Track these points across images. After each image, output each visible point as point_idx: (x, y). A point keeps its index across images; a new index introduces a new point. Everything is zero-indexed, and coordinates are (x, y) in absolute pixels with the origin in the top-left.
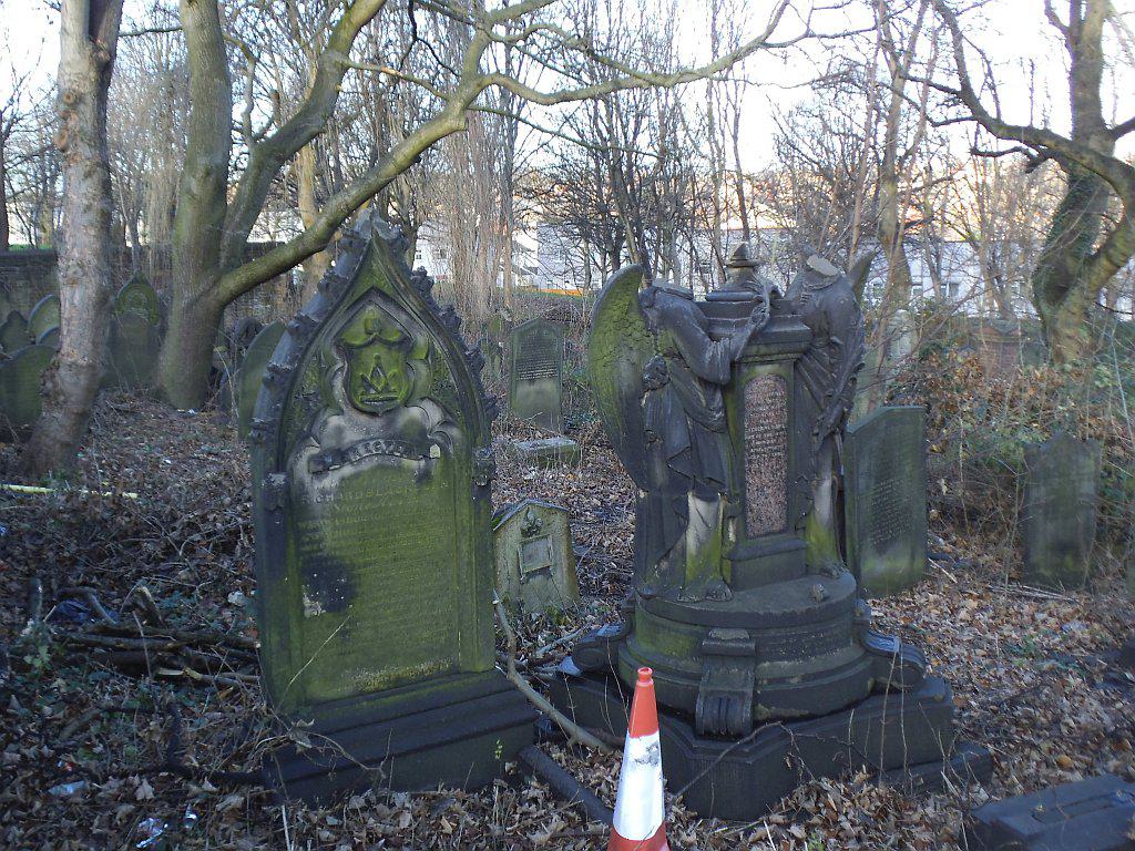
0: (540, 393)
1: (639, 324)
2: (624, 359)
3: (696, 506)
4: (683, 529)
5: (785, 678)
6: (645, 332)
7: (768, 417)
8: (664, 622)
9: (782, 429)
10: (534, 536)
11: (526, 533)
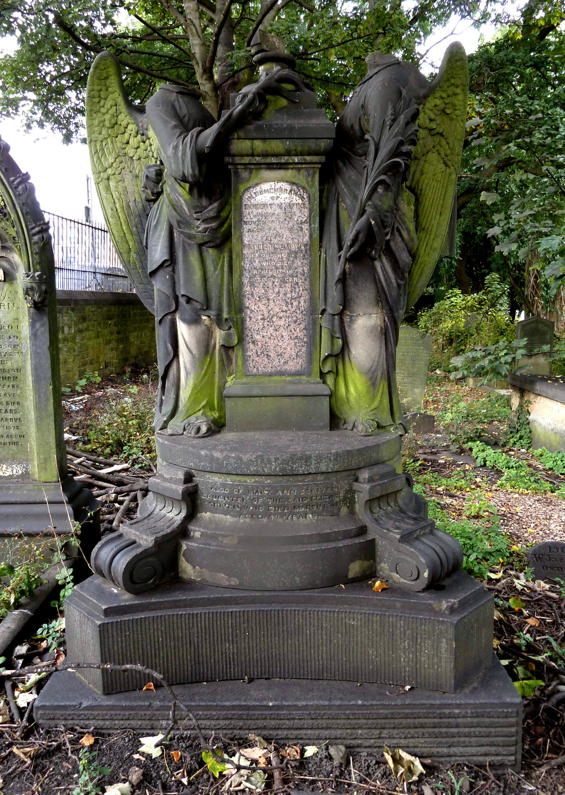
0: (535, 365)
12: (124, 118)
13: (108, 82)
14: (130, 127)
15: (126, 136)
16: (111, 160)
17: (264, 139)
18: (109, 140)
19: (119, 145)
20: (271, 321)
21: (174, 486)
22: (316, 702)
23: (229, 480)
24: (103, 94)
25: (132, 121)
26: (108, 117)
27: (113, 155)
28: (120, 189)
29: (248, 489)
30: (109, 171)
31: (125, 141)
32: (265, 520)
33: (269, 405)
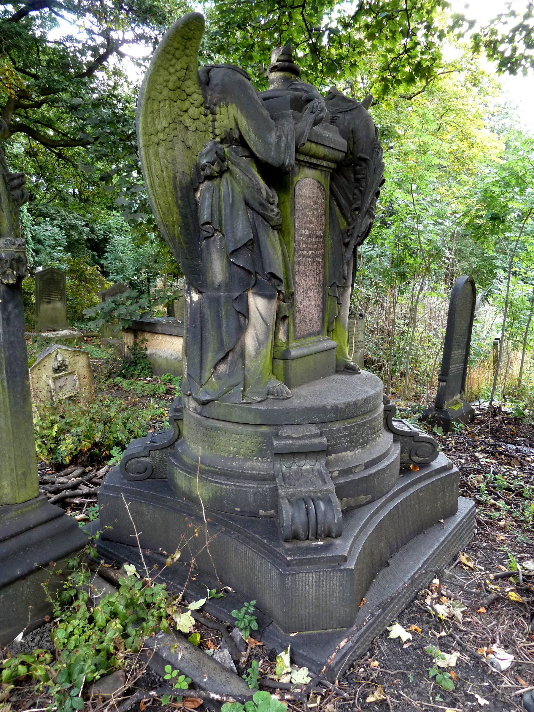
0: (54, 309)
1: (197, 98)
2: (179, 140)
3: (258, 305)
4: (241, 329)
5: (351, 468)
6: (202, 109)
7: (312, 222)
8: (221, 425)
10: (63, 373)
11: (56, 370)
14: (195, 96)
15: (187, 103)
18: (167, 102)
19: (177, 111)
20: (307, 293)
21: (315, 441)
25: (200, 91)
26: (174, 78)
27: (169, 119)
30: (161, 136)
31: (185, 109)
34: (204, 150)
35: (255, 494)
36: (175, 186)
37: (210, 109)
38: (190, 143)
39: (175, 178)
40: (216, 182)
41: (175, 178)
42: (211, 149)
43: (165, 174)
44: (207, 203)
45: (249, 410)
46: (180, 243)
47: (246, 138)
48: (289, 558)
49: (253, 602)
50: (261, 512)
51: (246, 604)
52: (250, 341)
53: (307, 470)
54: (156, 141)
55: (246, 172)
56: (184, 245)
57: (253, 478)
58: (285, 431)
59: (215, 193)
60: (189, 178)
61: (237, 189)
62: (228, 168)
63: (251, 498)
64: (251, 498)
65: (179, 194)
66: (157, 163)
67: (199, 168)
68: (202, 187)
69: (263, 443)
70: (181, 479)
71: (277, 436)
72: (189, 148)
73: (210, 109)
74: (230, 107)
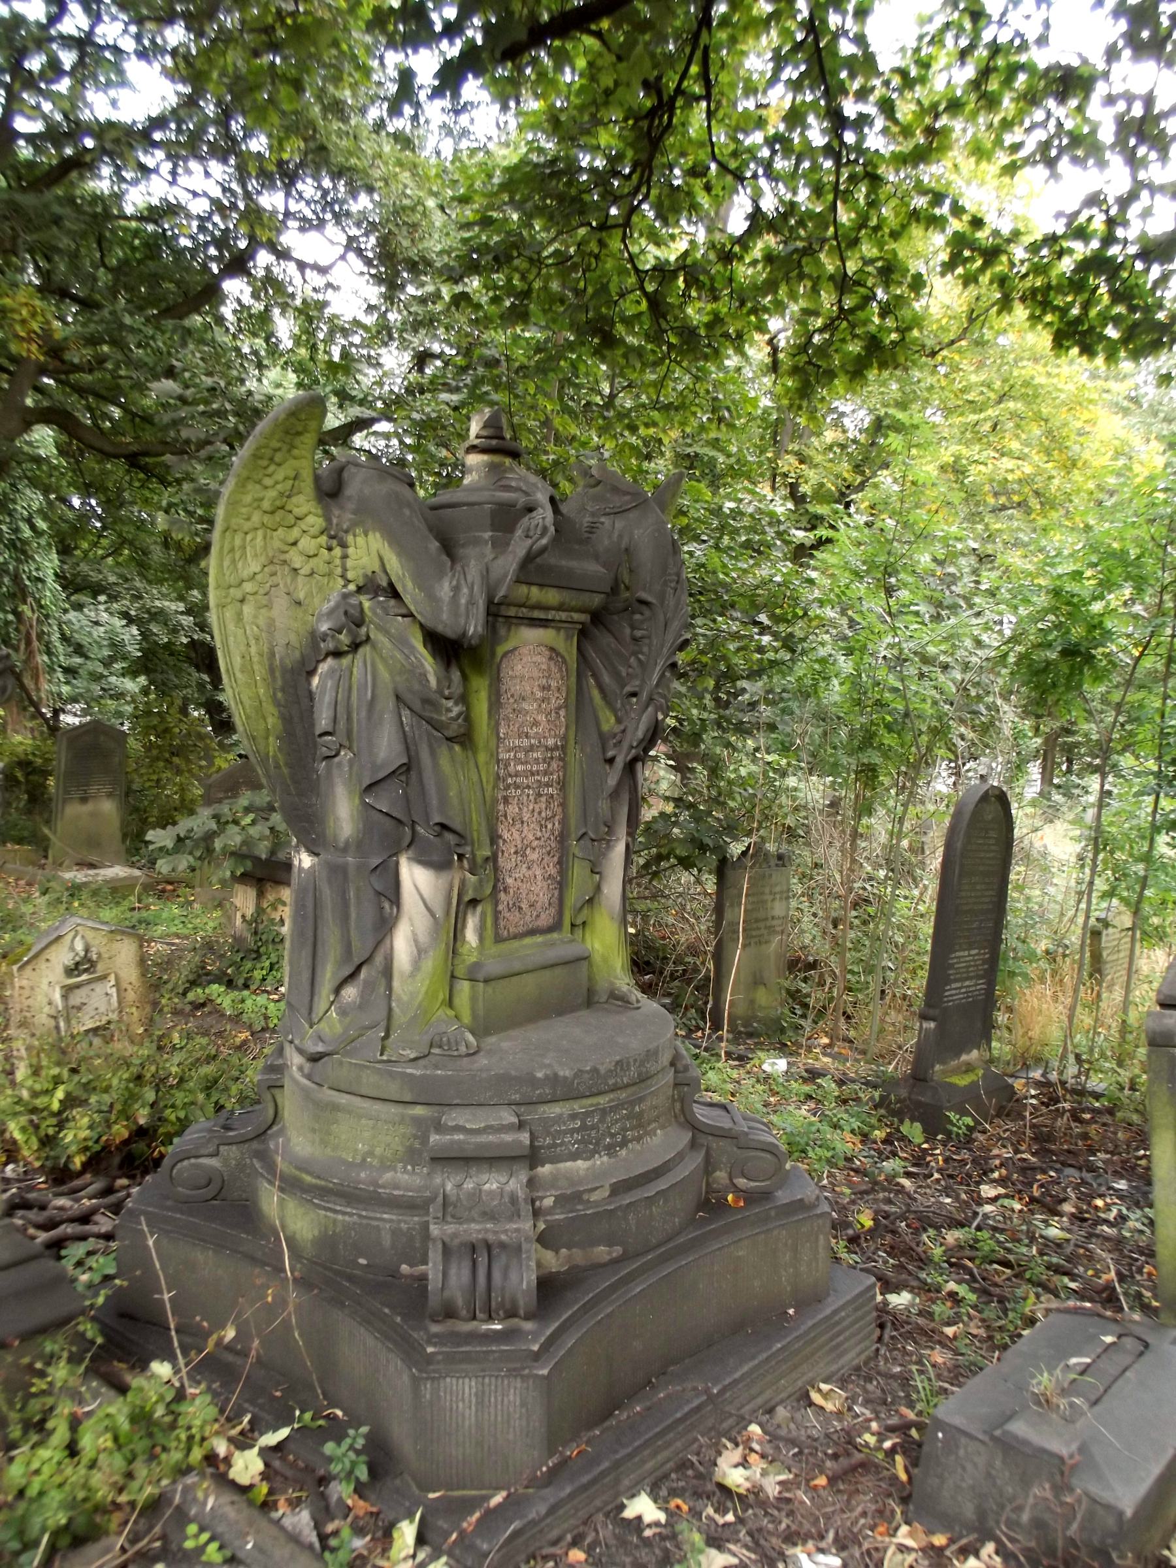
1: (315, 521)
3: (416, 879)
4: (385, 926)
6: (323, 539)
7: (536, 723)
8: (344, 1099)
9: (556, 748)
10: (84, 977)
11: (73, 970)
12: (304, 502)
13: (297, 441)
14: (311, 519)
15: (295, 533)
16: (255, 567)
17: (541, 586)
18: (260, 533)
19: (277, 544)
20: (524, 855)
21: (508, 1138)
22: (746, 1368)
23: (578, 1107)
24: (278, 457)
26: (272, 493)
28: (261, 621)
29: (604, 1112)
30: (248, 587)
32: (624, 1152)
33: (529, 985)
34: (326, 607)
35: (395, 1233)
36: (272, 670)
37: (337, 538)
38: (301, 595)
39: (272, 654)
40: (345, 661)
41: (272, 654)
42: (337, 606)
43: (253, 650)
44: (328, 698)
45: (391, 1074)
46: (277, 767)
47: (399, 589)
48: (430, 1350)
49: (364, 1430)
50: (405, 1268)
51: (351, 1432)
52: (402, 944)
53: (491, 1192)
54: (239, 596)
55: (401, 642)
56: (285, 770)
57: (393, 1203)
58: (454, 1118)
59: (342, 679)
60: (297, 654)
61: (384, 674)
62: (368, 638)
63: (387, 1241)
64: (387, 1241)
65: (279, 682)
66: (240, 632)
67: (315, 638)
68: (323, 668)
69: (415, 1137)
70: (272, 1202)
71: (439, 1128)
72: (299, 603)
73: (337, 538)
74: (371, 536)
